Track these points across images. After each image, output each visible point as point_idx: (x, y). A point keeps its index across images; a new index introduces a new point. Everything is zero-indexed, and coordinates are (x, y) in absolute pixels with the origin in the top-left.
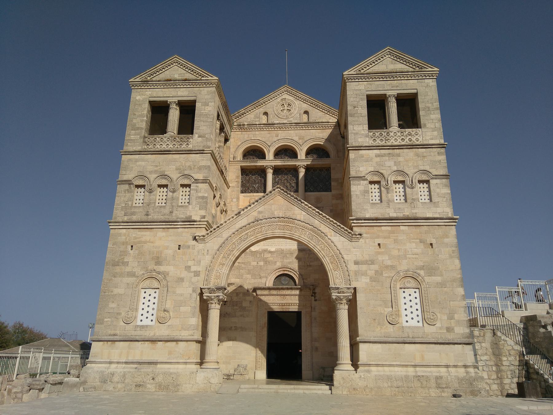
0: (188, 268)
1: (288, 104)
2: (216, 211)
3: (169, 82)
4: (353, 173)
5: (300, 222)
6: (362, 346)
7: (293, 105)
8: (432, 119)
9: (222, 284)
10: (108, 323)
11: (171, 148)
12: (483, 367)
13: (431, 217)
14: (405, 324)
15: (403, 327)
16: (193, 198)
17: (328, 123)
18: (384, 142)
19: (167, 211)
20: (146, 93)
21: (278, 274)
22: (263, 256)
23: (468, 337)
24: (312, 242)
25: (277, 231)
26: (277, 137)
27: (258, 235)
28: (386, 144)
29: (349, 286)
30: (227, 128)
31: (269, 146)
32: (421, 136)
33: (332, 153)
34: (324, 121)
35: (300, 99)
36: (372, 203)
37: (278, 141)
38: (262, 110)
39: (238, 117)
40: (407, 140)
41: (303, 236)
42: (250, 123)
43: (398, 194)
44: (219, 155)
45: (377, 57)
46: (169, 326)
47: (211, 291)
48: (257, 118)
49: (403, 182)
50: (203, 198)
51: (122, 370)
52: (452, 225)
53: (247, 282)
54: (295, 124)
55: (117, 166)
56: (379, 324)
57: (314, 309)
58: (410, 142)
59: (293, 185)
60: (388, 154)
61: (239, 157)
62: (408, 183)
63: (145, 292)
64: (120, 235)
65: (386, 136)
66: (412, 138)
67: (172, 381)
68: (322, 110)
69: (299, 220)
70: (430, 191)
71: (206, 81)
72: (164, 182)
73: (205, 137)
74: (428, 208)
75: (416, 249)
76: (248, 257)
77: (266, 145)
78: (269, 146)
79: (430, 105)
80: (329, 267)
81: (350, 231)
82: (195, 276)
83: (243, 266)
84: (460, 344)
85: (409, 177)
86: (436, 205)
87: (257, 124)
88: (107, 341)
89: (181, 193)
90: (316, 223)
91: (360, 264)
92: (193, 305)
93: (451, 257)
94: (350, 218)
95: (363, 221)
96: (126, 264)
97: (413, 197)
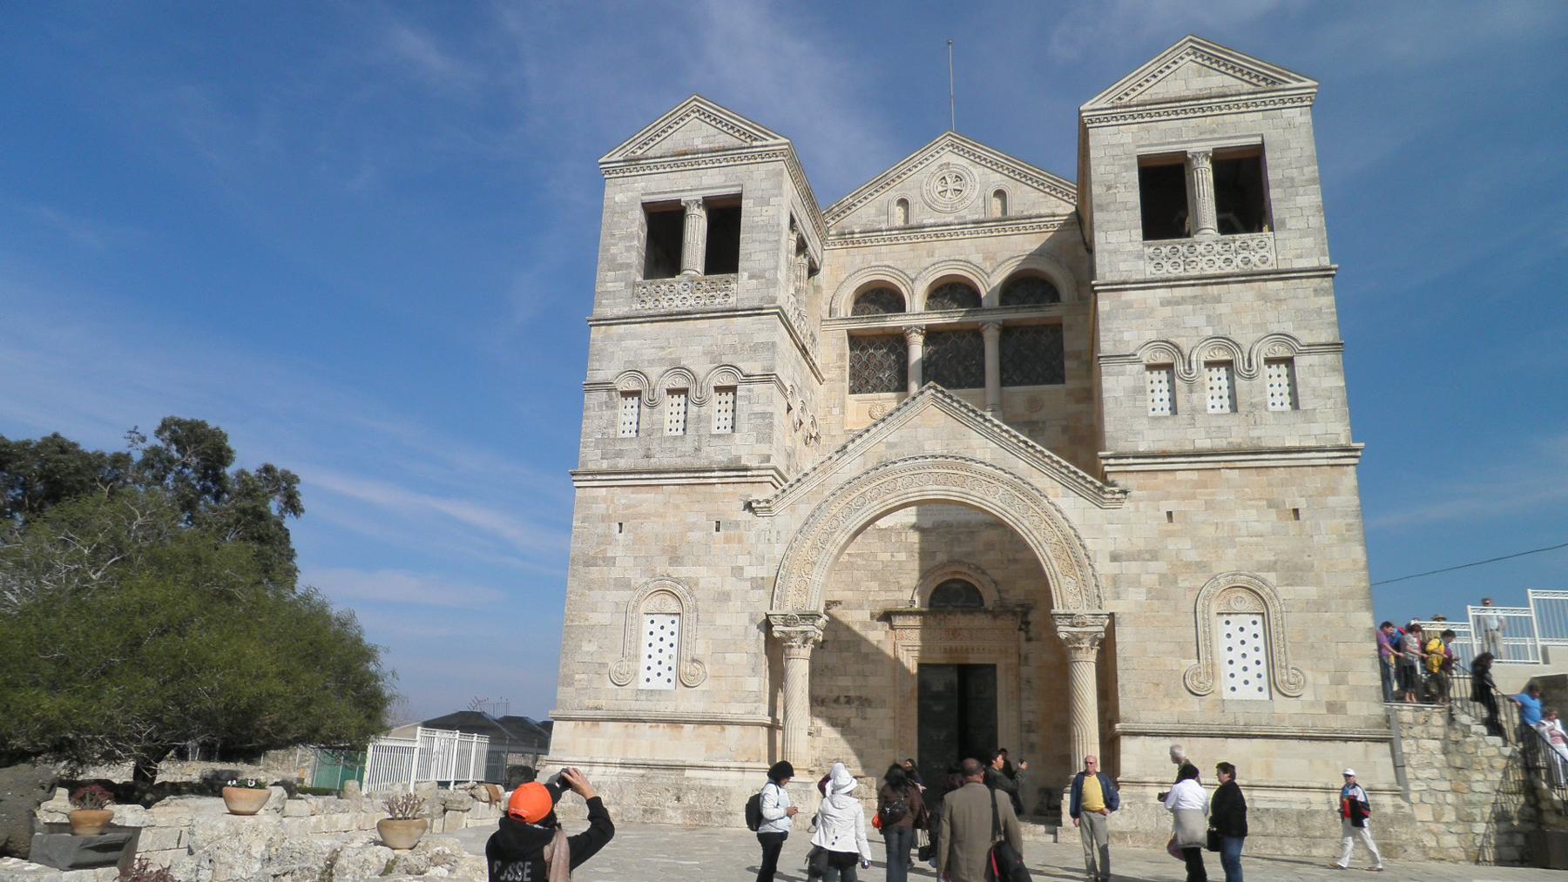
0: (737, 571)
1: (956, 177)
2: (793, 440)
3: (684, 158)
4: (1106, 346)
5: (982, 466)
6: (1126, 744)
7: (967, 176)
8: (1301, 208)
9: (813, 604)
10: (582, 682)
11: (691, 305)
12: (1421, 795)
13: (1294, 447)
14: (1227, 695)
15: (1224, 700)
16: (742, 416)
17: (1054, 216)
18: (1182, 267)
19: (688, 446)
20: (636, 184)
21: (939, 581)
22: (904, 540)
23: (1379, 725)
24: (1012, 512)
25: (929, 487)
26: (931, 259)
27: (889, 496)
28: (1187, 274)
29: (1097, 611)
30: (814, 245)
31: (913, 281)
32: (1273, 250)
33: (1065, 289)
34: (1043, 211)
35: (983, 162)
36: (1151, 417)
37: (933, 267)
38: (894, 194)
39: (838, 215)
40: (1238, 261)
41: (990, 499)
42: (868, 228)
43: (1216, 393)
44: (797, 312)
45: (1163, 61)
46: (704, 692)
47: (787, 620)
48: (884, 214)
49: (1228, 364)
50: (764, 415)
51: (615, 779)
52: (1348, 465)
53: (870, 598)
54: (974, 223)
55: (579, 354)
56: (1167, 695)
57: (1026, 658)
58: (1246, 267)
59: (973, 370)
60: (1191, 297)
61: (845, 306)
62: (1240, 365)
63: (652, 622)
64: (595, 500)
65: (1187, 254)
66: (1251, 257)
67: (716, 805)
68: (1039, 185)
69: (981, 462)
70: (1293, 384)
71: (762, 149)
72: (680, 383)
73: (763, 277)
74: (1289, 425)
75: (1257, 524)
76: (869, 541)
77: (905, 278)
78: (913, 281)
79: (1295, 173)
80: (1053, 566)
81: (1099, 484)
82: (753, 588)
83: (860, 561)
84: (1360, 740)
85: (1242, 352)
86: (1310, 417)
87: (884, 228)
88: (583, 720)
89: (718, 407)
90: (1020, 466)
91: (1126, 561)
92: (753, 650)
93: (1343, 540)
94: (1099, 453)
95: (1131, 461)
96: (611, 562)
97: (1254, 401)
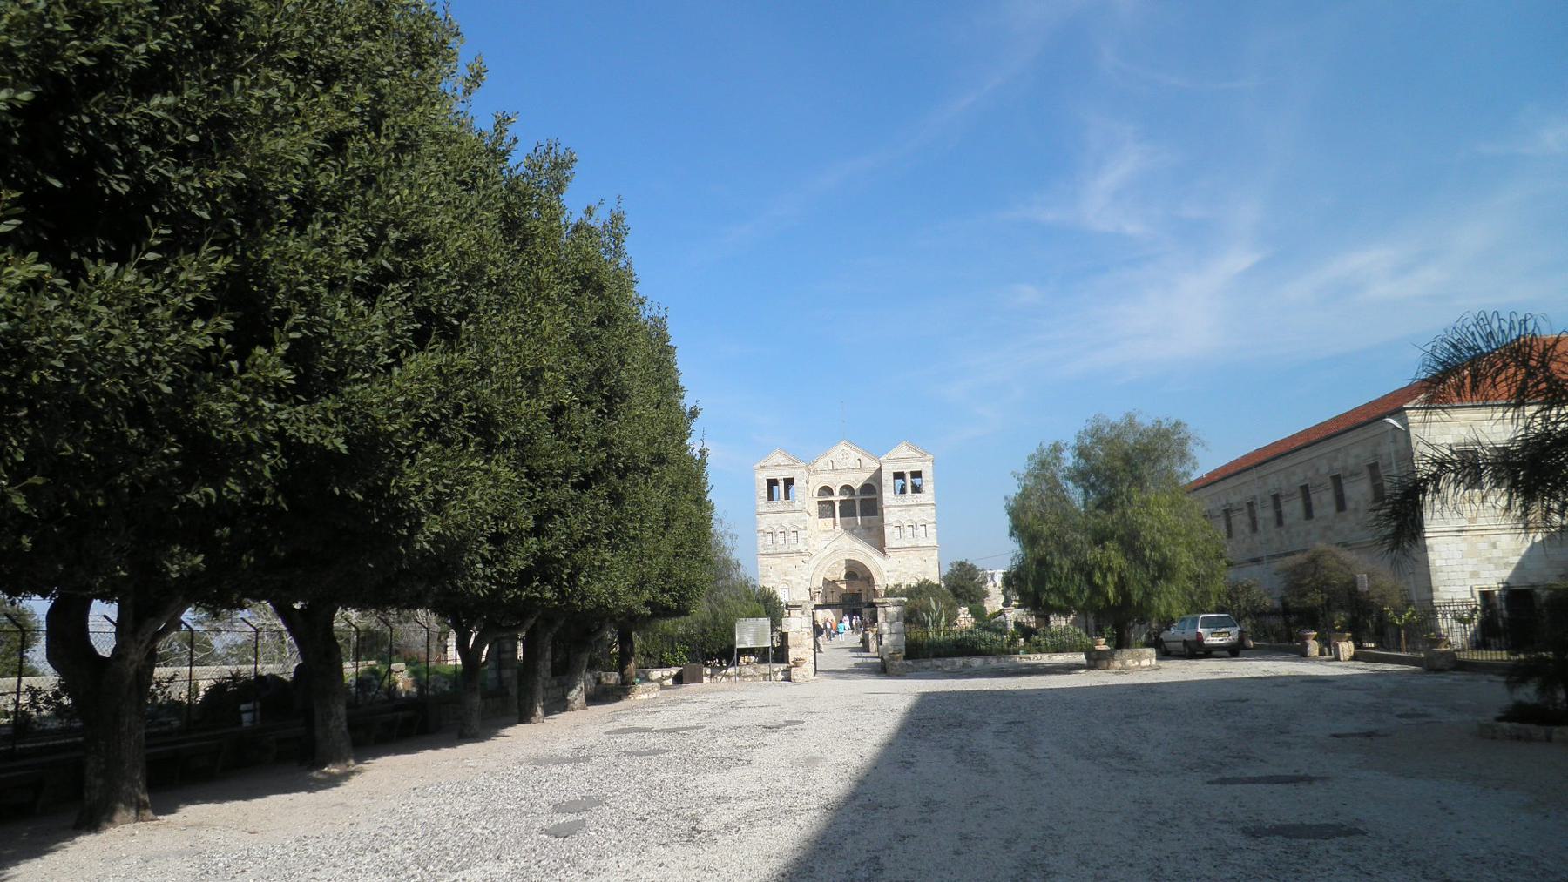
38: (828, 458)
